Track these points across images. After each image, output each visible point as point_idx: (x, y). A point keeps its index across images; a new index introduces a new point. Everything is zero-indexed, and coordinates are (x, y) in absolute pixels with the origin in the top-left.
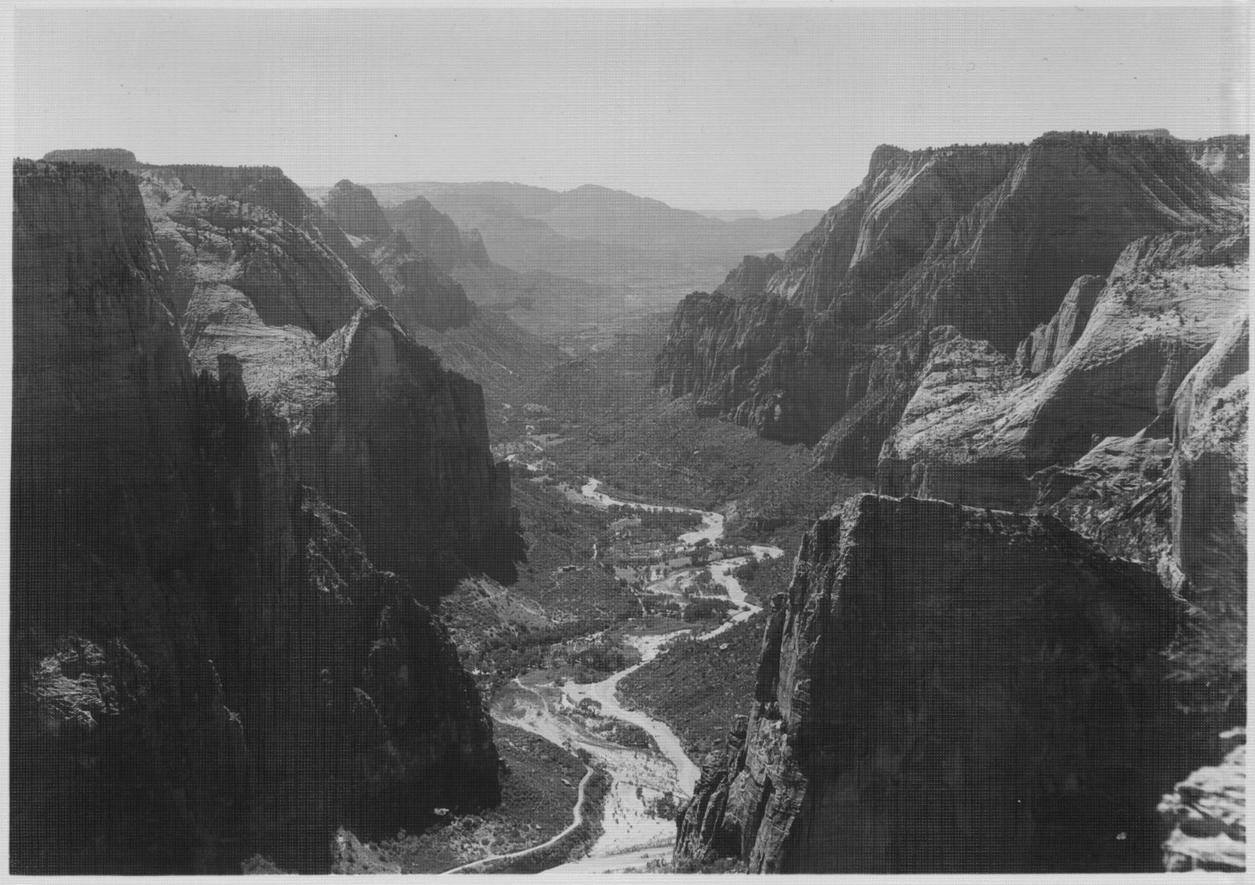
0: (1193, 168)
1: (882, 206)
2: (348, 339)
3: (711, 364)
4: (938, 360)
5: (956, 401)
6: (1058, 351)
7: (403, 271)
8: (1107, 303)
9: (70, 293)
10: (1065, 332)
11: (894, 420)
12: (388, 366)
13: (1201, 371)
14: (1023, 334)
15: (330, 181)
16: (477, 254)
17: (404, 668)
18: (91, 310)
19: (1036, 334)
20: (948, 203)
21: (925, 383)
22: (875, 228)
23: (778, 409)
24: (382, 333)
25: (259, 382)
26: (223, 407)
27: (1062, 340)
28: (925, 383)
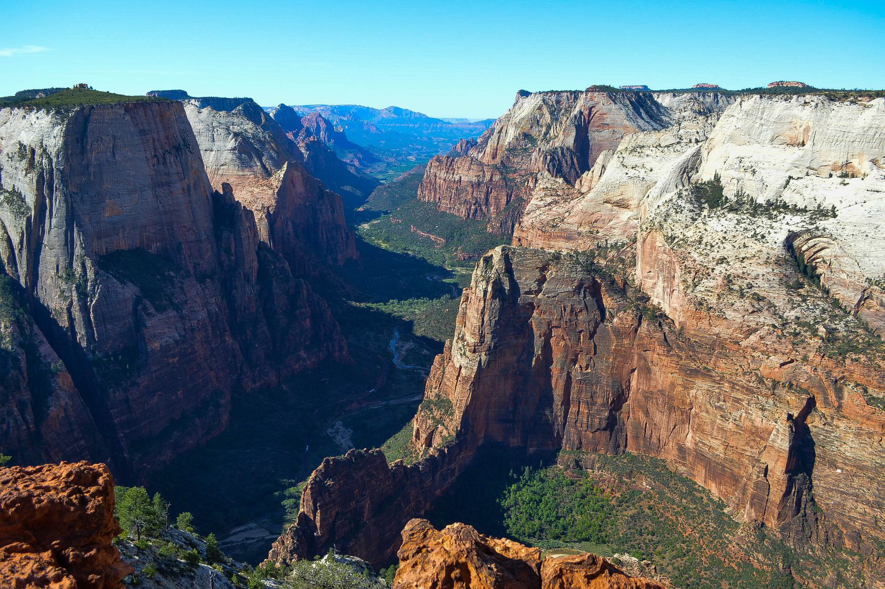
0: (656, 104)
1: (519, 118)
2: (282, 176)
3: (444, 187)
4: (541, 186)
5: (549, 204)
6: (593, 183)
7: (308, 147)
8: (613, 164)
9: (155, 156)
10: (596, 178)
11: (520, 214)
12: (300, 188)
13: (654, 192)
14: (578, 176)
15: (276, 105)
16: (340, 139)
17: (308, 320)
18: (165, 163)
19: (584, 175)
20: (548, 116)
21: (536, 197)
22: (517, 126)
23: (473, 207)
24: (296, 173)
25: (241, 196)
26: (224, 208)
27: (596, 178)
28: (536, 197)
